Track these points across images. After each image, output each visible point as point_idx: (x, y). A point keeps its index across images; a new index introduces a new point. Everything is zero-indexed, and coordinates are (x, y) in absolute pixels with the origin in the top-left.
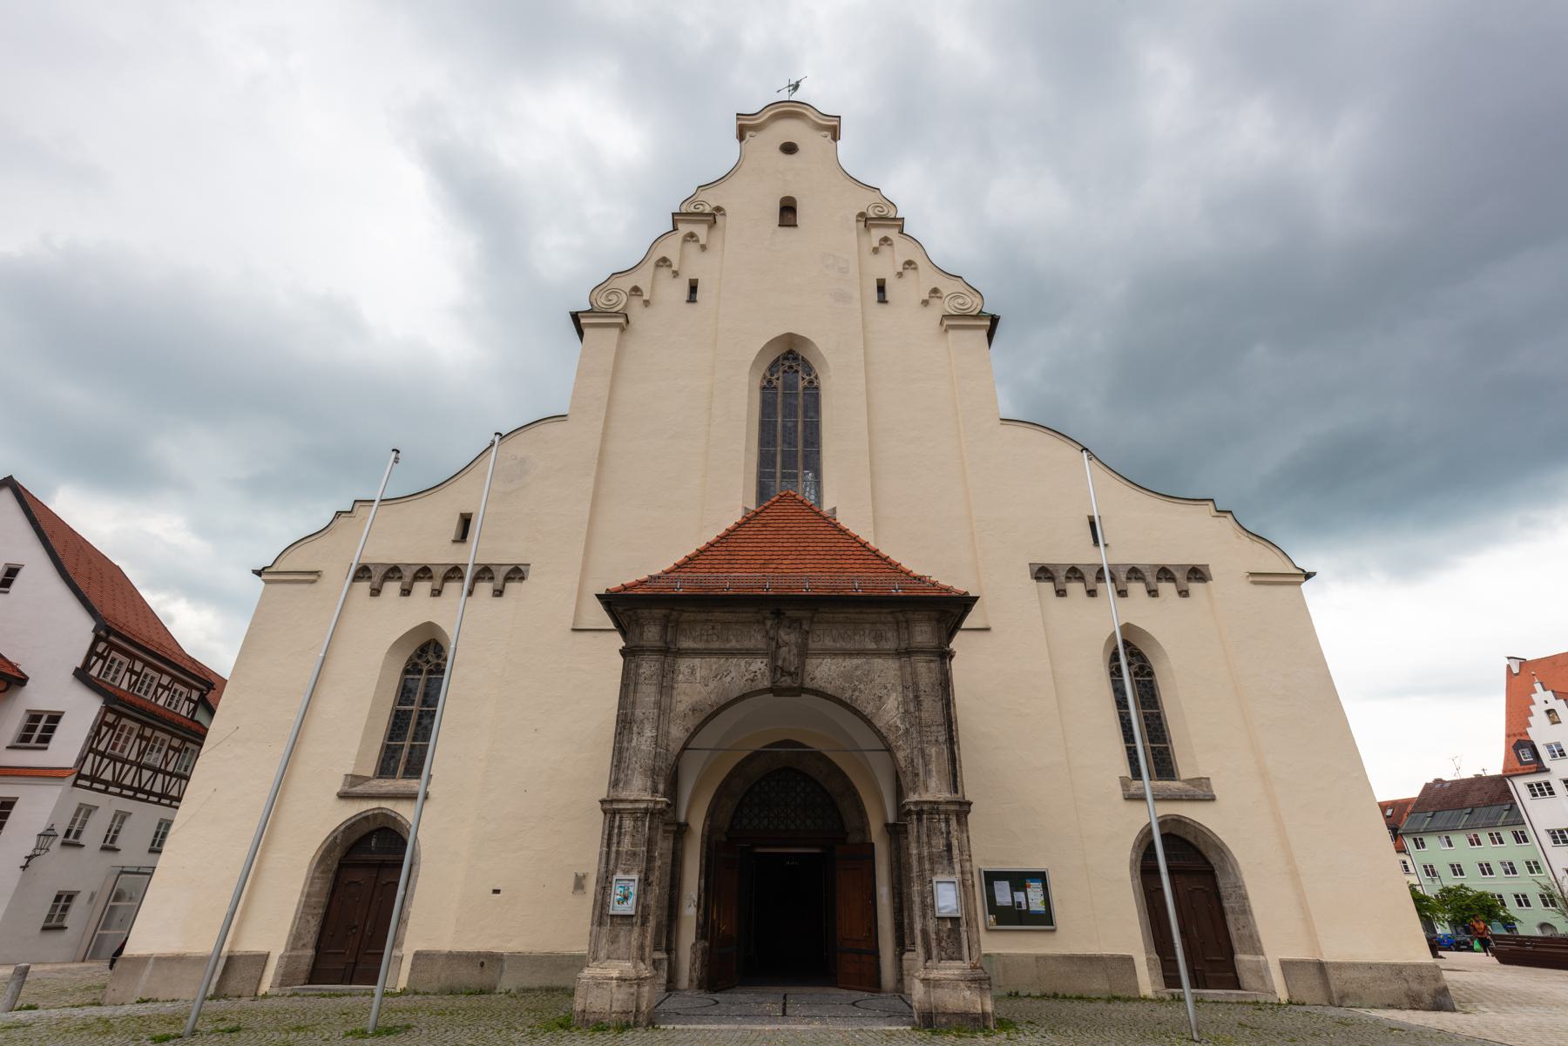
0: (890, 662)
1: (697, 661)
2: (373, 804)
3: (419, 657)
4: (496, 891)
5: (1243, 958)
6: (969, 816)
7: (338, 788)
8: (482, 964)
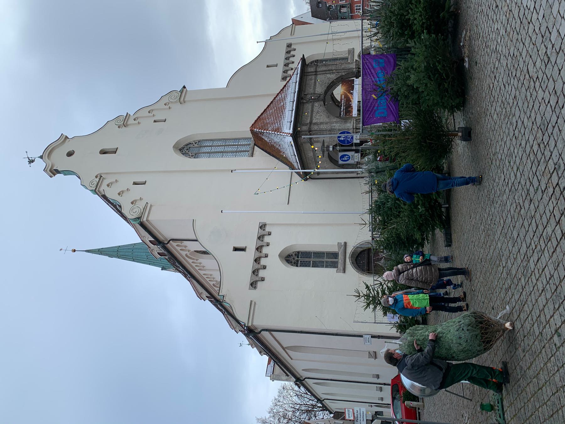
0: (318, 77)
3: (291, 262)
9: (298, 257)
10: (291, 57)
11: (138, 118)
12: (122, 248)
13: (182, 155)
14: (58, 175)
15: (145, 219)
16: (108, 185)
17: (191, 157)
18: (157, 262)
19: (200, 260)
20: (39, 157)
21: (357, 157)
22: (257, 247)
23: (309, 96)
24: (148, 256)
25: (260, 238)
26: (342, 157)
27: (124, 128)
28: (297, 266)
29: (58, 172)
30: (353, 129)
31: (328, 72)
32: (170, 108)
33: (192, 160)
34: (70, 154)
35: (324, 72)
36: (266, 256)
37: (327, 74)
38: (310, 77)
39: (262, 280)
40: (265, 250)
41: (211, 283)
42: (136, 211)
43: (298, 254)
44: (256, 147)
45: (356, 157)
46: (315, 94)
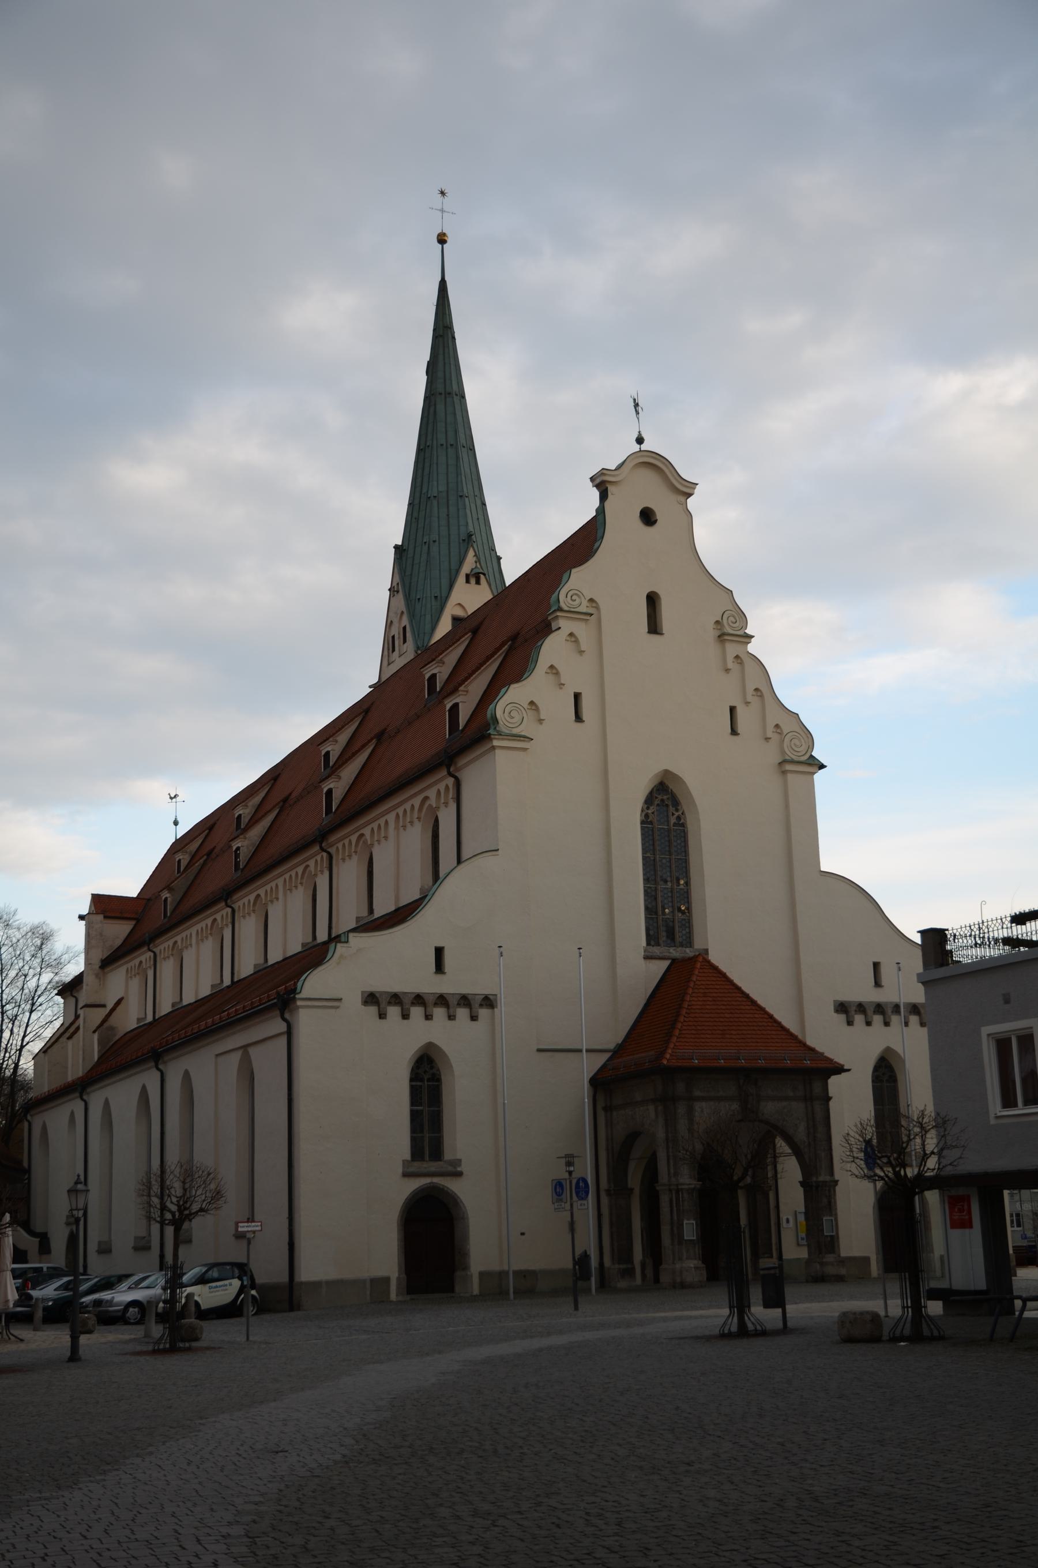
1: (704, 1104)
4: (523, 1234)
6: (837, 1188)
7: (400, 1170)
8: (525, 1276)
9: (429, 1080)
11: (741, 663)
12: (458, 407)
13: (650, 789)
14: (595, 494)
15: (495, 743)
16: (571, 635)
19: (418, 827)
20: (639, 432)
22: (445, 995)
25: (465, 1000)
27: (712, 633)
28: (411, 1080)
29: (604, 496)
30: (677, 1185)
32: (767, 739)
34: (648, 517)
36: (428, 1017)
40: (439, 1013)
41: (367, 831)
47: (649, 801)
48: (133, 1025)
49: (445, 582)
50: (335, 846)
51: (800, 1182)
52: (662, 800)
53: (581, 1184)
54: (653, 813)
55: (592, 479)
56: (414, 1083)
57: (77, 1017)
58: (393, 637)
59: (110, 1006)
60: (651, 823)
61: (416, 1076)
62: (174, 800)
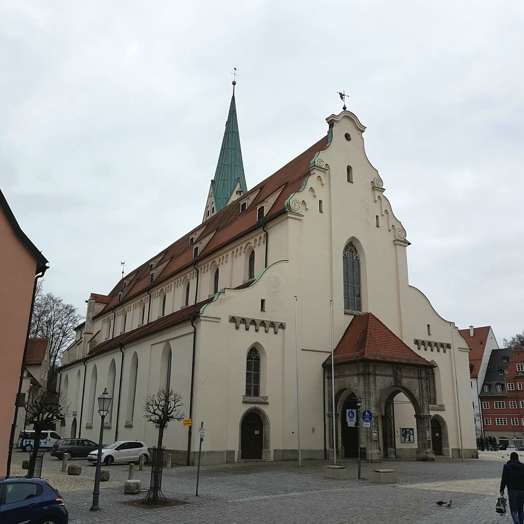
0: (417, 380)
2: (253, 405)
3: (250, 353)
4: (293, 433)
5: (444, 448)
10: (438, 348)
15: (289, 215)
17: (344, 253)
18: (221, 176)
19: (243, 256)
20: (344, 105)
21: (352, 424)
22: (264, 321)
23: (399, 373)
24: (227, 166)
25: (273, 324)
26: (353, 413)
27: (370, 187)
28: (247, 359)
31: (421, 389)
32: (390, 230)
33: (342, 256)
35: (420, 386)
37: (419, 388)
38: (417, 373)
39: (236, 327)
40: (262, 329)
42: (296, 206)
43: (258, 359)
44: (353, 316)
45: (352, 423)
46: (401, 378)
47: (346, 248)
48: (103, 340)
49: (229, 193)
50: (200, 267)
51: (414, 415)
52: (351, 249)
53: (366, 414)
54: (347, 254)
55: (327, 119)
56: (248, 360)
57: (81, 338)
58: (208, 211)
59: (94, 334)
60: (346, 258)
61: (249, 358)
62: (123, 264)
